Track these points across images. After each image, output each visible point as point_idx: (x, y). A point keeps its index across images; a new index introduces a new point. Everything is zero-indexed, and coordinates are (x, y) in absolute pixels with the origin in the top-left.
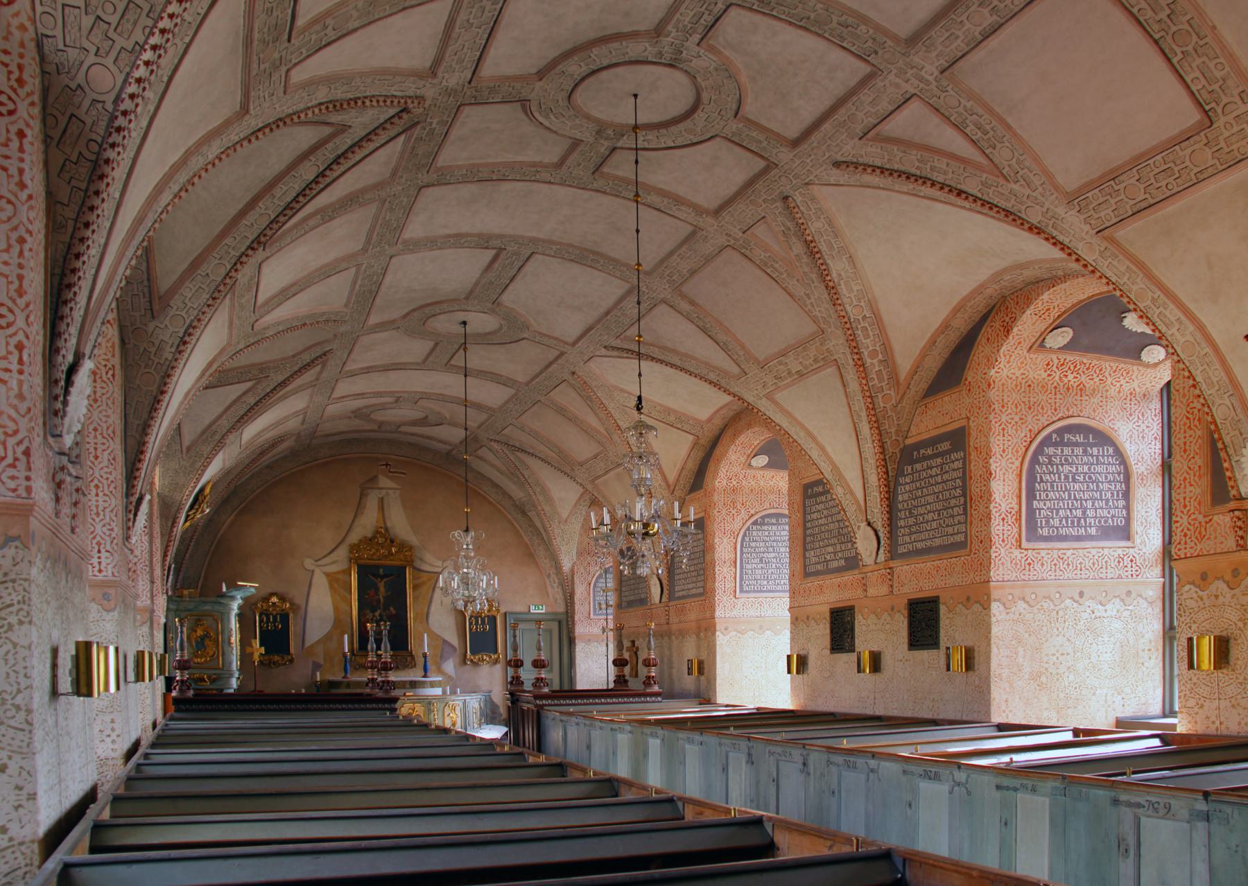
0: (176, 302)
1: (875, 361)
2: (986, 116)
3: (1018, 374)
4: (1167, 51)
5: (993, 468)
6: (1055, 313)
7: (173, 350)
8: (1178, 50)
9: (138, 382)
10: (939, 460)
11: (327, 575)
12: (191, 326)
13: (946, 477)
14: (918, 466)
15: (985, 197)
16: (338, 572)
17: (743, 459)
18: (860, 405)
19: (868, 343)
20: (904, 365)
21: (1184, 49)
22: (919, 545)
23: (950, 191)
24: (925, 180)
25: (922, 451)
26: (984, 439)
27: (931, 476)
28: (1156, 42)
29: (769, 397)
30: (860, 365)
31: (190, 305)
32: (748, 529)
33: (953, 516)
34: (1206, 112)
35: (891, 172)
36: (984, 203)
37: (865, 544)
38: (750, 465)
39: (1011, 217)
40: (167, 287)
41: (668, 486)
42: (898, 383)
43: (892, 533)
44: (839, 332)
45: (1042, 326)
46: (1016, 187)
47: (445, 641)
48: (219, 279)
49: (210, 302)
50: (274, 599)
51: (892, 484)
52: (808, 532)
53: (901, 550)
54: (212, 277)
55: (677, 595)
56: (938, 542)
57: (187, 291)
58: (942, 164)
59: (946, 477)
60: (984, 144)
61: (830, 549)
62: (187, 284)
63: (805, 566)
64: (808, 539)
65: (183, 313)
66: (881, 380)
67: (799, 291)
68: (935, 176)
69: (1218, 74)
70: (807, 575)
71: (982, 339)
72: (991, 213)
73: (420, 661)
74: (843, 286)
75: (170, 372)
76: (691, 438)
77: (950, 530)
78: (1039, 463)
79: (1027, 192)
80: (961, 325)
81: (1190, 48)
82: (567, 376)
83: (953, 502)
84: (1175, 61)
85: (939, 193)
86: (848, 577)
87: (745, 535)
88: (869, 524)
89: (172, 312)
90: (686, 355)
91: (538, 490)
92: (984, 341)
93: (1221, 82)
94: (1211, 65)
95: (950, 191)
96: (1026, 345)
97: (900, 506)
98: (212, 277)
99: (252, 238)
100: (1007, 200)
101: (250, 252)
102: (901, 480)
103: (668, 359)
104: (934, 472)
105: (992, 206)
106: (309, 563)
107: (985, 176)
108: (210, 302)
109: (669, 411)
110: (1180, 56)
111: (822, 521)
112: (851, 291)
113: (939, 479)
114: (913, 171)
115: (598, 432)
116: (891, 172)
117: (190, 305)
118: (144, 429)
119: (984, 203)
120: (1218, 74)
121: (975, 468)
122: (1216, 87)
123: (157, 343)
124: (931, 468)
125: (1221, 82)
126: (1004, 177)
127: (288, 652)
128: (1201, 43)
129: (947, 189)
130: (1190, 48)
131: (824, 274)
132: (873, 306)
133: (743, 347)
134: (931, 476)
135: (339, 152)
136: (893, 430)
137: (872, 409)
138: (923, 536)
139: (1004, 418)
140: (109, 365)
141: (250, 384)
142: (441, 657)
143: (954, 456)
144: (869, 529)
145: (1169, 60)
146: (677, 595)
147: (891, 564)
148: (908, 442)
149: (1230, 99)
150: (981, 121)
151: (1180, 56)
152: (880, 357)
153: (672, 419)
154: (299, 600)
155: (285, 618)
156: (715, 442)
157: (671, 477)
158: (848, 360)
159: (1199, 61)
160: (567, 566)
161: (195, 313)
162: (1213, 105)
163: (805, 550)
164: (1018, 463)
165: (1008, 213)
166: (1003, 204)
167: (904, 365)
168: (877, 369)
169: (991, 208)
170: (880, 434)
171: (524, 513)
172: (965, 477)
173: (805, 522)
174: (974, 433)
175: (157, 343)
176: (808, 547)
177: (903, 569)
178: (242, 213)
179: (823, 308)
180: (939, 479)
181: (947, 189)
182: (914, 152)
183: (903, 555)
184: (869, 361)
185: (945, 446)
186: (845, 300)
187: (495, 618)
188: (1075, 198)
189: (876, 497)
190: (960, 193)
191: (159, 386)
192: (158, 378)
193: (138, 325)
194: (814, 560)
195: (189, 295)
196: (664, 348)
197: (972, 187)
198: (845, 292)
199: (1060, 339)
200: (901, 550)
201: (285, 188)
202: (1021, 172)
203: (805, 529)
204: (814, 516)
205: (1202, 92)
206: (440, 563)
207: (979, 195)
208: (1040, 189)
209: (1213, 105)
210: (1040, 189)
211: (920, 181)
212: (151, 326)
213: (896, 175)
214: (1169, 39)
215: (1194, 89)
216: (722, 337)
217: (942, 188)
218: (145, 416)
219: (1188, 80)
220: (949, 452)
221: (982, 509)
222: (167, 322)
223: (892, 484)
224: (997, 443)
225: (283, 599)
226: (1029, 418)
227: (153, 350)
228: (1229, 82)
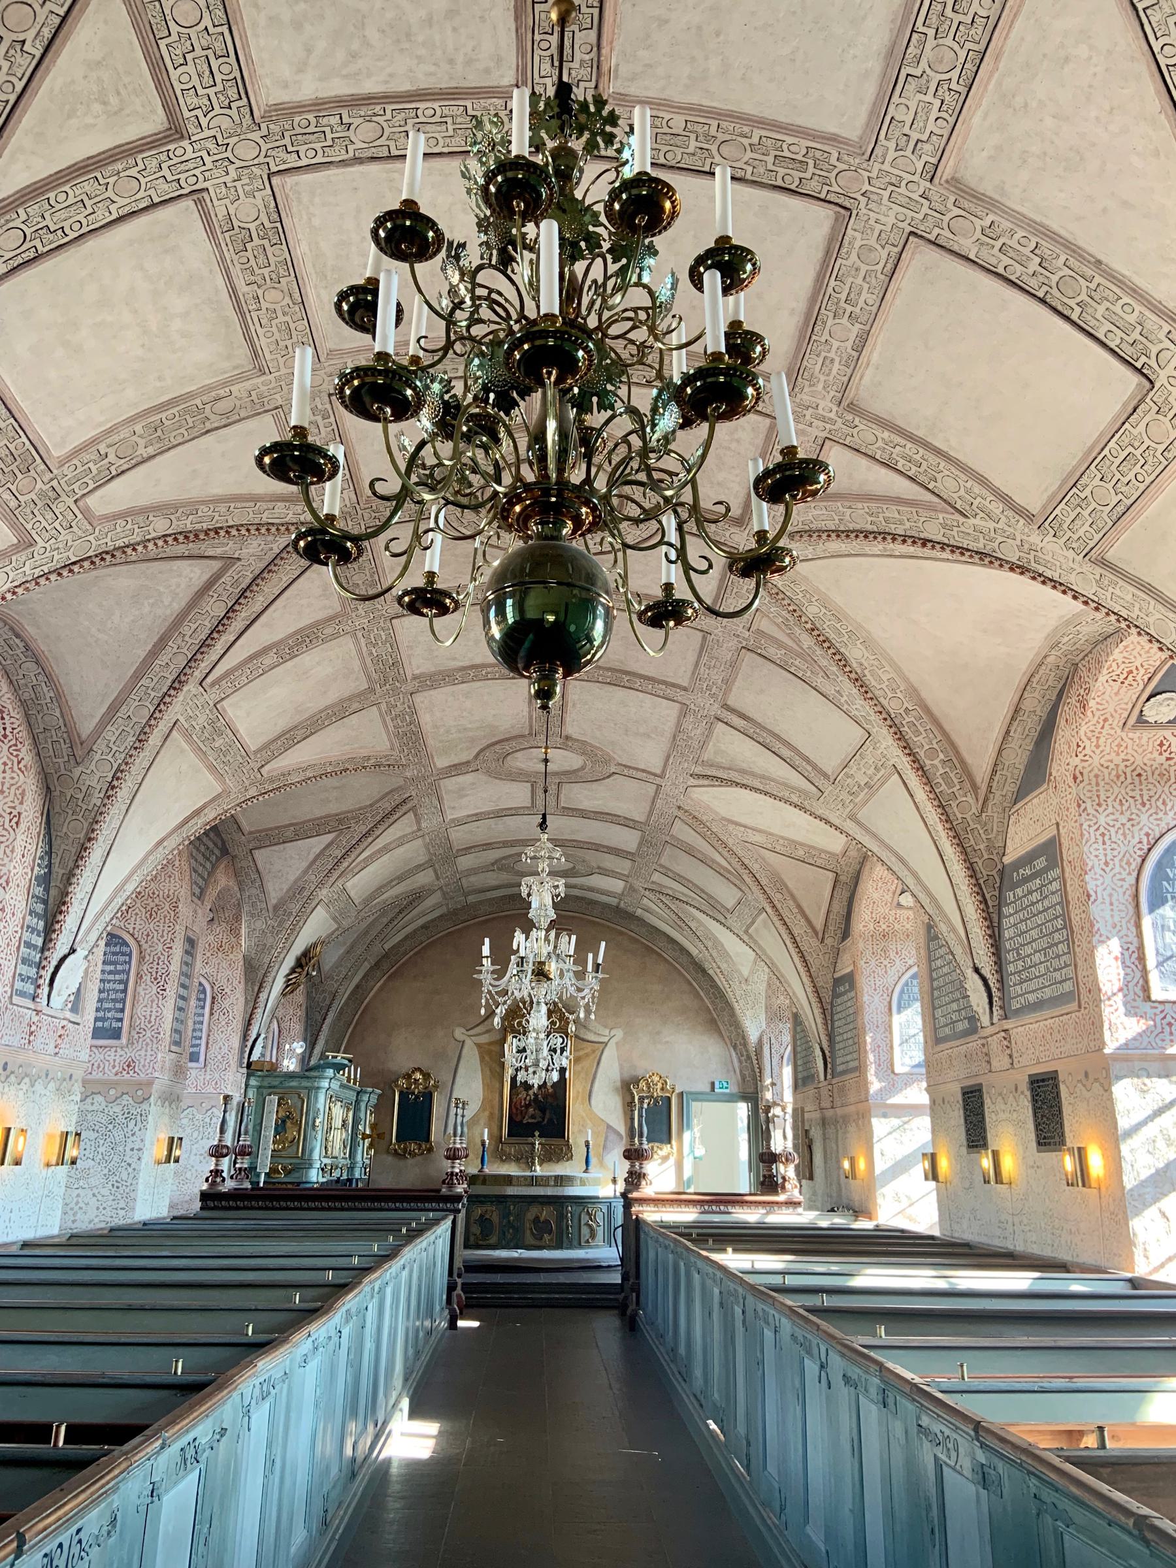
0: (100, 746)
1: (936, 762)
2: (909, 445)
3: (1117, 760)
4: (1060, 308)
5: (1091, 887)
6: (1142, 677)
7: (102, 795)
8: (1072, 303)
9: (64, 830)
10: (1038, 881)
11: (478, 1046)
12: (118, 770)
13: (1046, 903)
14: (1019, 891)
15: (952, 542)
16: (491, 1044)
17: (888, 897)
18: (933, 816)
19: (922, 741)
20: (981, 767)
21: (1078, 299)
22: (1032, 998)
23: (914, 542)
24: (883, 535)
25: (1021, 871)
26: (1076, 848)
27: (1033, 904)
28: (1043, 301)
29: (852, 817)
30: (920, 769)
31: (115, 749)
32: (906, 984)
33: (1058, 956)
34: (1139, 371)
35: (847, 533)
36: (954, 548)
37: (977, 998)
38: (899, 904)
39: (987, 560)
40: (89, 732)
41: (816, 933)
42: (975, 787)
43: (1001, 981)
44: (885, 731)
45: (1129, 695)
46: (977, 521)
47: (609, 1127)
48: (144, 721)
49: (137, 744)
50: (418, 1076)
51: (995, 917)
52: (935, 984)
53: (1015, 1005)
54: (135, 720)
55: (840, 1069)
56: (1048, 993)
57: (111, 733)
58: (892, 512)
59: (1046, 903)
60: (921, 478)
61: (954, 1006)
62: (109, 728)
63: (935, 1029)
64: (936, 993)
65: (109, 757)
66: (950, 784)
67: (830, 690)
68: (892, 528)
69: (1132, 318)
70: (938, 1041)
71: (1061, 722)
72: (963, 559)
73: (579, 1152)
74: (869, 677)
75: (99, 818)
76: (831, 875)
77: (1057, 975)
78: (1168, 879)
79: (992, 525)
80: (1035, 705)
81: (1083, 297)
82: (676, 812)
83: (1056, 935)
84: (1074, 317)
85: (912, 549)
86: (973, 1044)
87: (902, 992)
88: (977, 970)
89: (97, 757)
90: (763, 777)
91: (710, 944)
92: (1063, 722)
93: (1139, 328)
94: (1117, 309)
95: (914, 542)
96: (1117, 722)
97: (1008, 946)
98: (135, 720)
99: (171, 678)
100: (976, 540)
101: (172, 692)
102: (1005, 910)
103: (749, 783)
104: (1035, 897)
105: (963, 550)
106: (459, 1033)
107: (941, 516)
108: (137, 744)
109: (795, 844)
110: (1078, 310)
111: (945, 970)
112: (881, 681)
113: (1040, 907)
114: (870, 528)
115: (729, 872)
116: (847, 533)
117: (115, 749)
118: (69, 879)
119: (954, 548)
120: (1132, 318)
121: (1073, 894)
122: (1136, 335)
123: (84, 789)
124: (1030, 892)
125: (1139, 328)
126: (961, 513)
127: (427, 1139)
128: (1093, 286)
129: (910, 541)
130: (1083, 297)
131: (843, 662)
132: (913, 692)
133: (808, 760)
134: (1033, 904)
135: (244, 586)
136: (982, 847)
137: (947, 819)
138: (1033, 985)
139: (1102, 820)
140: (15, 813)
141: (330, 837)
142: (605, 1147)
143: (1052, 874)
144: (976, 977)
145: (1067, 318)
146: (840, 1069)
147: (1007, 1024)
148: (1007, 860)
149: (1161, 346)
150: (907, 451)
151: (1078, 310)
152: (942, 756)
153: (801, 853)
154: (445, 1077)
155: (429, 1096)
156: (857, 879)
157: (819, 924)
158: (904, 763)
159: (1101, 309)
160: (753, 1036)
161: (123, 756)
162: (1143, 359)
163: (934, 1008)
164: (1132, 880)
165: (982, 555)
166: (973, 546)
167: (981, 767)
168: (942, 771)
169: (962, 554)
170: (964, 852)
171: (704, 971)
172: (1065, 902)
173: (931, 971)
174: (1065, 842)
175: (84, 789)
176: (936, 1002)
177: (1024, 1030)
178: (154, 653)
179: (861, 707)
180: (1040, 907)
181: (910, 541)
182: (860, 505)
183: (1017, 1012)
184: (928, 762)
185: (1041, 863)
186: (877, 693)
187: (669, 1099)
188: (1044, 521)
189: (978, 932)
190: (925, 542)
191: (87, 833)
192: (86, 825)
193: (63, 772)
194: (943, 1021)
195: (113, 739)
196: (743, 772)
197: (933, 531)
198: (874, 683)
199: (1164, 709)
200: (1015, 1005)
201: (194, 626)
202: (976, 503)
203: (932, 980)
204: (939, 963)
205: (1124, 346)
206: (606, 1032)
207: (946, 541)
208: (1003, 519)
209: (1143, 359)
210: (1003, 519)
211: (880, 538)
212: (77, 772)
213: (853, 535)
214: (1055, 291)
215: (1112, 345)
216: (786, 753)
217: (904, 541)
218: (71, 864)
219: (1101, 336)
220: (1046, 870)
221: (1085, 945)
222: (92, 767)
223: (996, 919)
224: (1094, 854)
225: (427, 1076)
226: (1144, 818)
227: (81, 796)
228: (1148, 325)
